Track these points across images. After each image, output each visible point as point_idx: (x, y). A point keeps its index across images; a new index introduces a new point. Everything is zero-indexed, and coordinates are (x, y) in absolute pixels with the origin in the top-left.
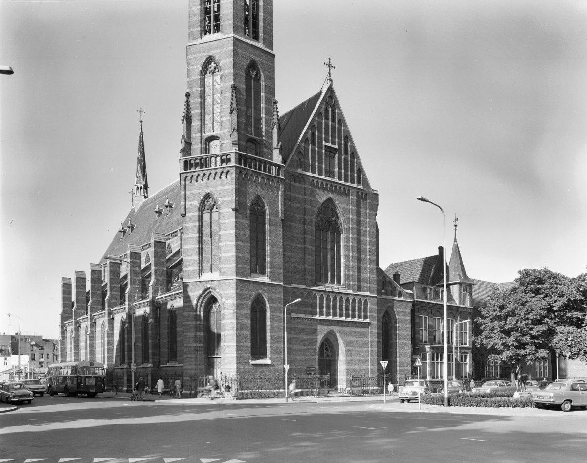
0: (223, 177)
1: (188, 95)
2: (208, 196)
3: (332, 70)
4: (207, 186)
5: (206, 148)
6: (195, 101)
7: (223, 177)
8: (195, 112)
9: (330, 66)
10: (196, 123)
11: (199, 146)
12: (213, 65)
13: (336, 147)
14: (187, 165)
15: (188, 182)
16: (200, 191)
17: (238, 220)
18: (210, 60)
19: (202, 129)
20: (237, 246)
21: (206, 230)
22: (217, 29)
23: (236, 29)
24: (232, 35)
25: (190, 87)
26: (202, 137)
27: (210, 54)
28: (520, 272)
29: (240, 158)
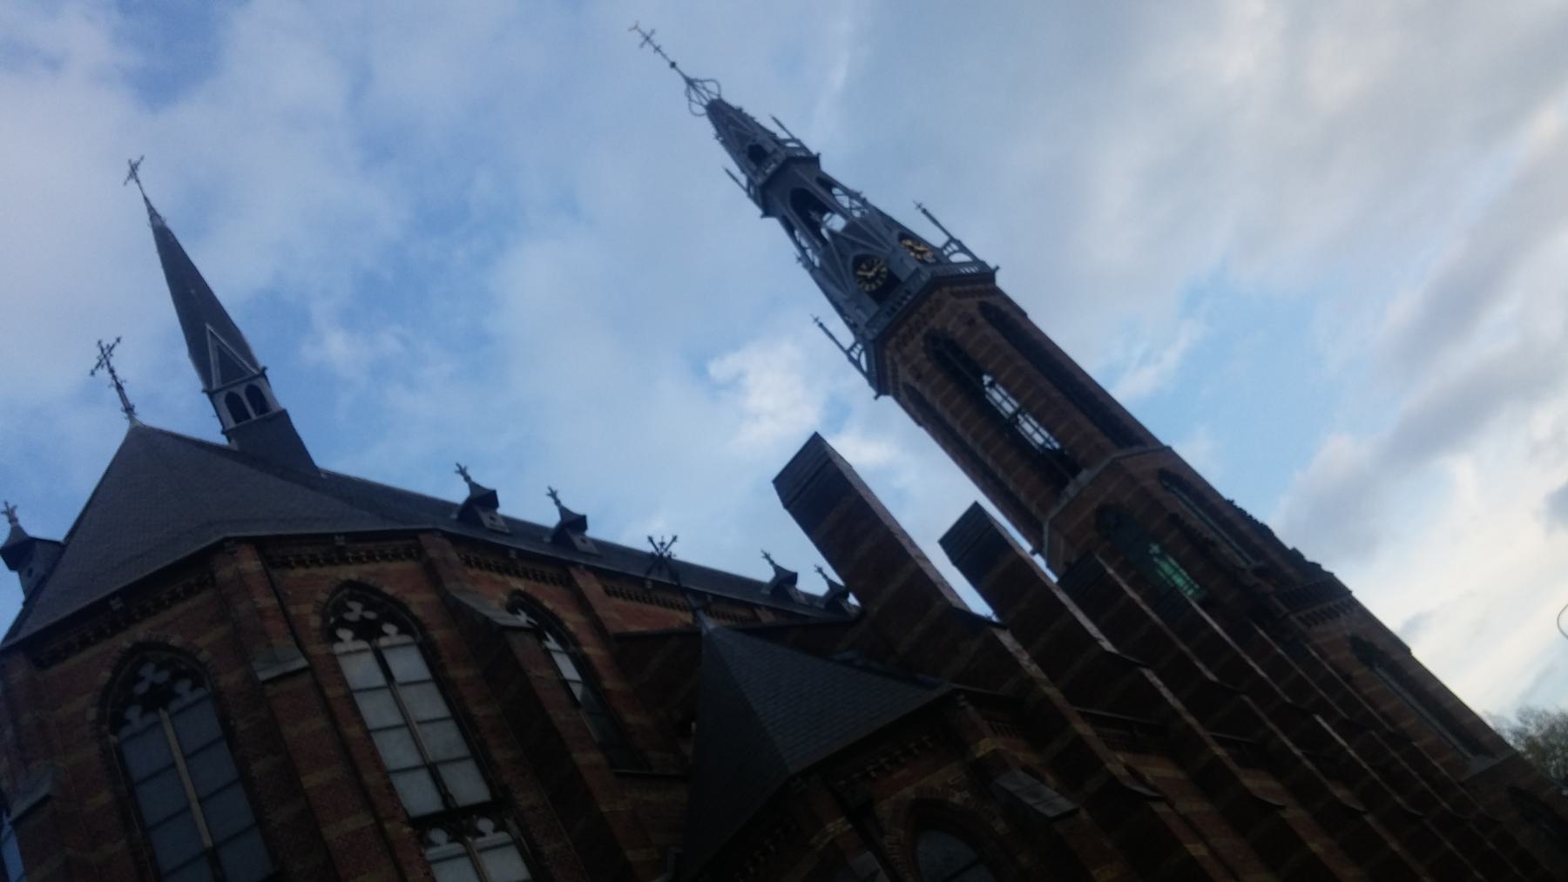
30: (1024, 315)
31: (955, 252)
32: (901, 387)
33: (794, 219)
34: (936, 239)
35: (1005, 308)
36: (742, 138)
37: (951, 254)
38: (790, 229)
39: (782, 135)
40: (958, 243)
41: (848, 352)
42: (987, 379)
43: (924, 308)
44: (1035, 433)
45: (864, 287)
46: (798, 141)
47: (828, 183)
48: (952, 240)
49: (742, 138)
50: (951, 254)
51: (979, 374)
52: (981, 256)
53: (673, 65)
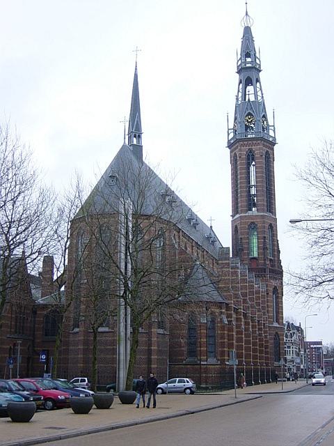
33: (243, 82)
34: (271, 123)
35: (271, 156)
36: (248, 48)
38: (240, 82)
39: (257, 55)
42: (254, 163)
43: (254, 142)
44: (253, 191)
47: (258, 80)
49: (248, 48)
51: (253, 160)
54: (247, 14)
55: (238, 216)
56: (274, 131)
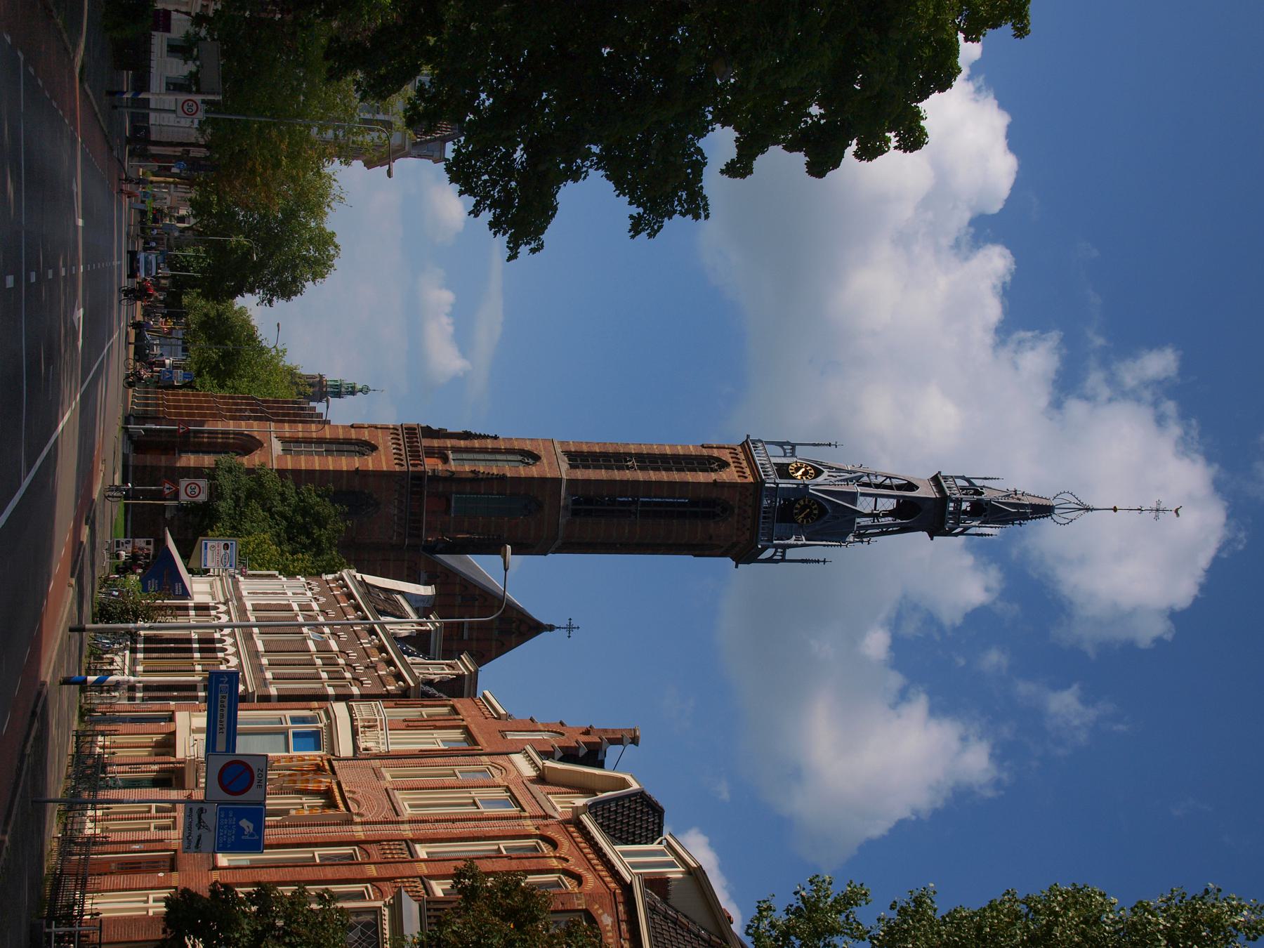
0: (396, 461)
1: (496, 438)
2: (374, 448)
3: (564, 633)
4: (386, 447)
5: (434, 453)
6: (489, 444)
7: (396, 461)
8: (476, 443)
9: (570, 628)
10: (462, 443)
11: (436, 445)
12: (531, 461)
13: (466, 636)
14: (411, 431)
15: (391, 431)
16: (381, 441)
17: (345, 475)
18: (537, 458)
19: (456, 450)
20: (314, 471)
21: (334, 447)
22: (572, 467)
23: (571, 482)
24: (564, 476)
25: (504, 439)
26: (447, 448)
27: (544, 460)
28: (243, 296)
29: (418, 477)
30: (695, 556)
31: (774, 555)
32: (731, 461)
37: (776, 551)
40: (777, 561)
41: (793, 446)
45: (804, 501)
46: (956, 535)
48: (783, 560)
50: (776, 551)
52: (754, 566)
53: (1115, 509)
54: (1088, 509)
55: (564, 466)
56: (770, 560)
